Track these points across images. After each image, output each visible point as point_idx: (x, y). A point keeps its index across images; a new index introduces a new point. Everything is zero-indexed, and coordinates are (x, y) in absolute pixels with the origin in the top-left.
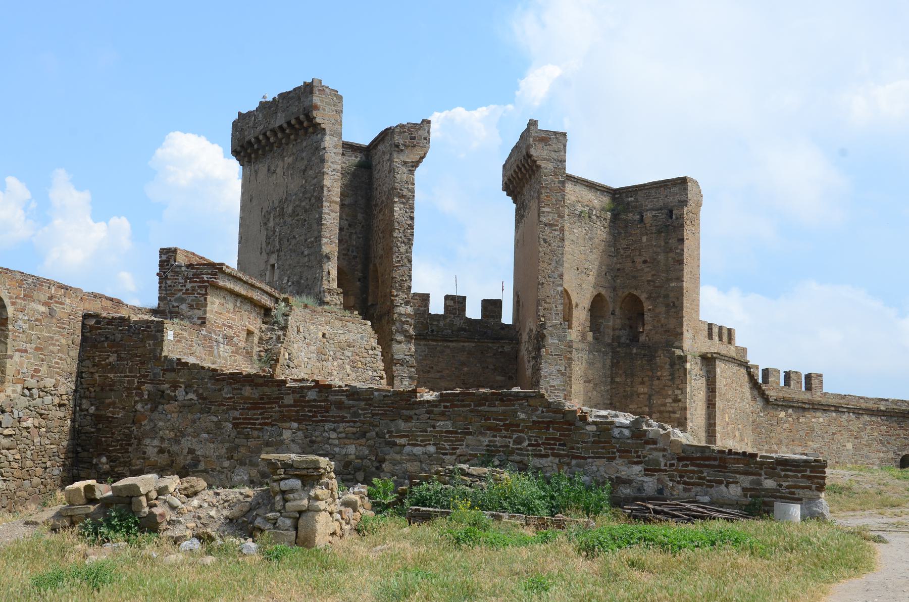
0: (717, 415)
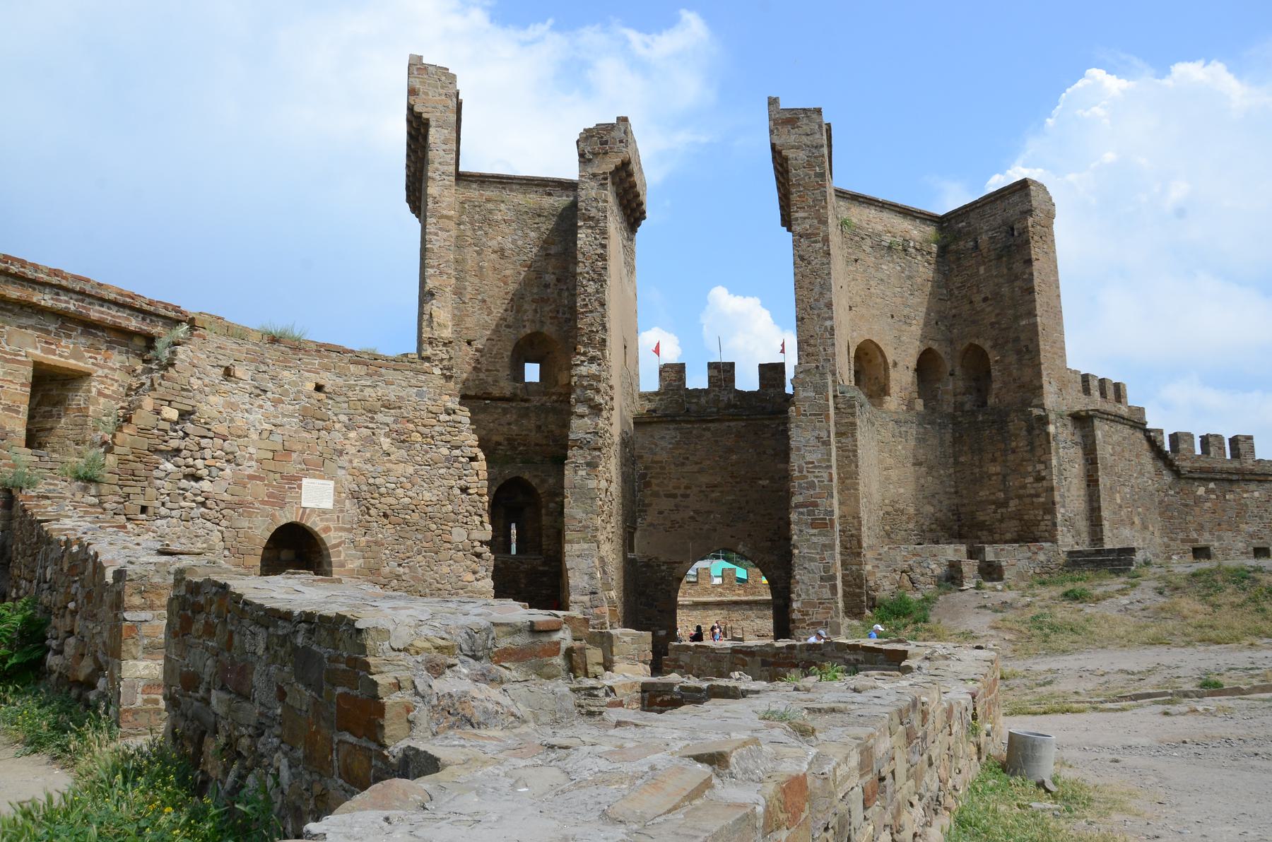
0: (1102, 496)
